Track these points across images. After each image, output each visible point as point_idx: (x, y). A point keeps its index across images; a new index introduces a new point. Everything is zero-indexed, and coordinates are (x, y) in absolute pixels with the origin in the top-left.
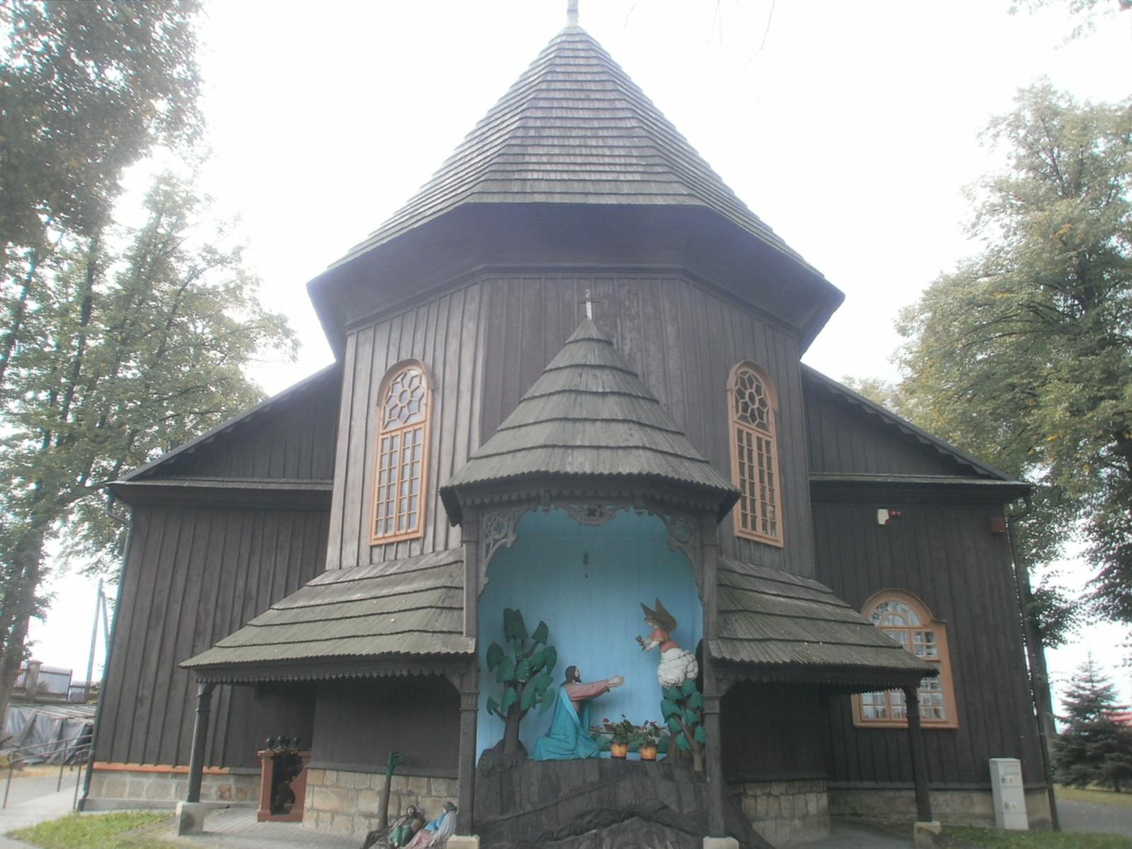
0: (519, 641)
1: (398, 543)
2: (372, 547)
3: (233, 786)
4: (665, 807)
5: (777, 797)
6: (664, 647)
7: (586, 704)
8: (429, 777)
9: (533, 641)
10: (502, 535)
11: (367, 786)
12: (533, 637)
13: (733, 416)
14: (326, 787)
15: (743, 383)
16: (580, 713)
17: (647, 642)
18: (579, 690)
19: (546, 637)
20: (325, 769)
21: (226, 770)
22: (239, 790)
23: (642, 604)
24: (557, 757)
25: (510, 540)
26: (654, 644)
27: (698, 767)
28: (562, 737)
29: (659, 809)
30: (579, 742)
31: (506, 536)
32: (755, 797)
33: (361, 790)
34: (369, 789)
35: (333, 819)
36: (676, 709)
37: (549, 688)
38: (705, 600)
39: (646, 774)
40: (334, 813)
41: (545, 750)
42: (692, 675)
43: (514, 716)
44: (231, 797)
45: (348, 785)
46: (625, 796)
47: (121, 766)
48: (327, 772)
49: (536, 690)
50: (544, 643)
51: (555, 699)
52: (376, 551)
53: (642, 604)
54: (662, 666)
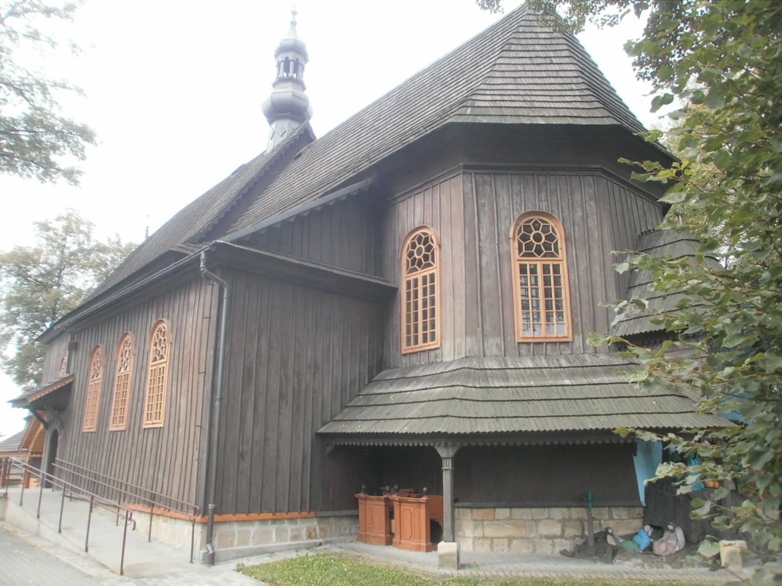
1: (547, 343)
2: (519, 343)
3: (317, 527)
11: (546, 516)
14: (499, 520)
20: (494, 508)
21: (312, 513)
22: (321, 529)
33: (540, 520)
34: (549, 518)
40: (510, 539)
44: (316, 536)
45: (524, 517)
47: (230, 517)
48: (474, 510)
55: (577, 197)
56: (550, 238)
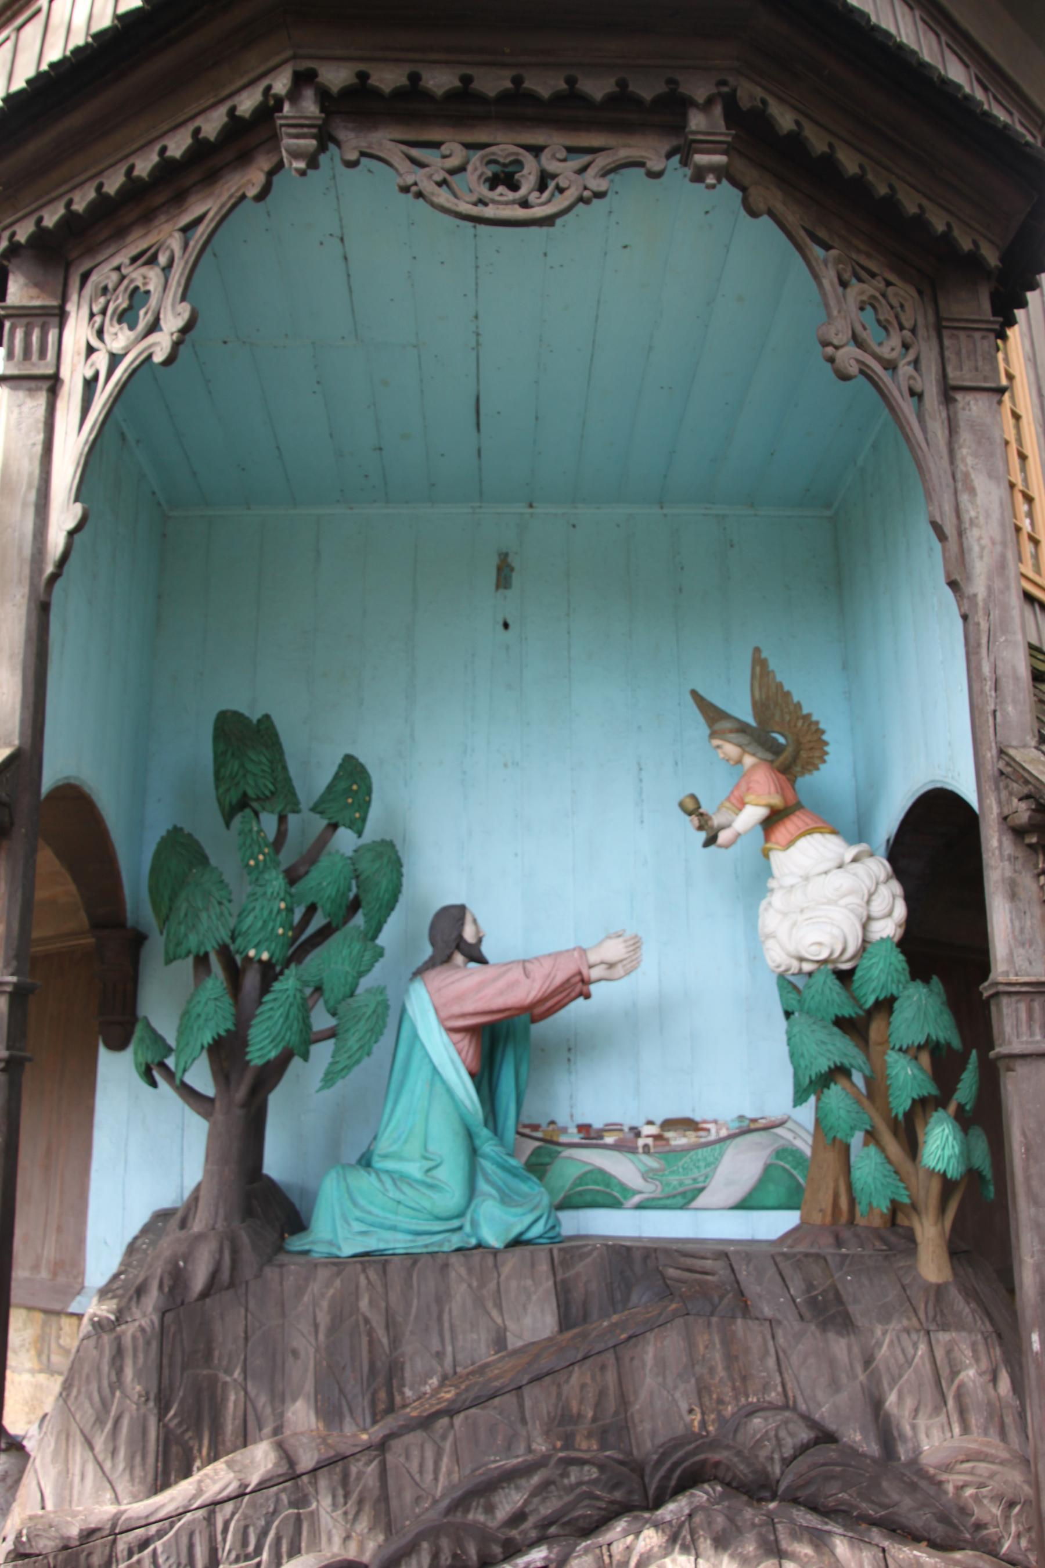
0: (269, 823)
4: (826, 1437)
6: (781, 833)
7: (496, 1043)
9: (321, 823)
10: (141, 326)
12: (313, 809)
16: (485, 1077)
17: (717, 820)
18: (477, 991)
19: (365, 806)
23: (694, 694)
24: (398, 1243)
25: (161, 345)
26: (752, 814)
27: (932, 1264)
28: (414, 1169)
29: (803, 1449)
30: (482, 1186)
31: (154, 327)
37: (365, 983)
38: (978, 587)
39: (743, 1306)
41: (346, 1221)
43: (242, 1093)
46: (665, 1392)
49: (318, 989)
50: (358, 827)
51: (387, 1018)
53: (694, 694)
54: (777, 899)
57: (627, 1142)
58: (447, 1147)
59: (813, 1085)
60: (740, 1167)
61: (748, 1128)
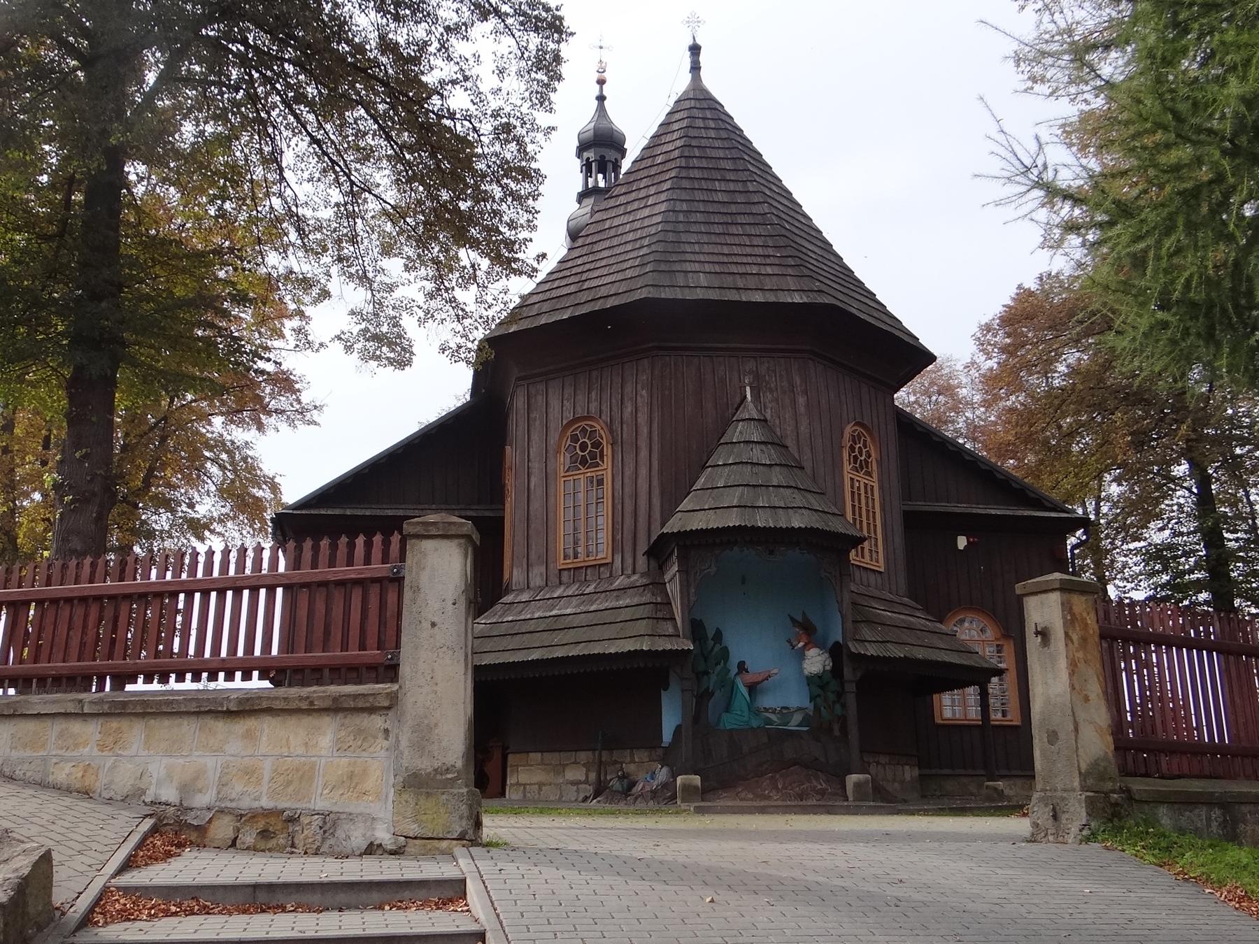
5: (884, 766)
7: (752, 688)
8: (632, 749)
13: (847, 467)
15: (854, 440)
18: (749, 678)
26: (801, 644)
27: (837, 733)
32: (869, 764)
34: (575, 763)
35: (540, 789)
36: (819, 691)
40: (541, 785)
42: (828, 668)
52: (565, 574)
55: (629, 389)
56: (597, 445)
57: (774, 711)
58: (746, 709)
59: (813, 698)
60: (797, 718)
61: (799, 709)
